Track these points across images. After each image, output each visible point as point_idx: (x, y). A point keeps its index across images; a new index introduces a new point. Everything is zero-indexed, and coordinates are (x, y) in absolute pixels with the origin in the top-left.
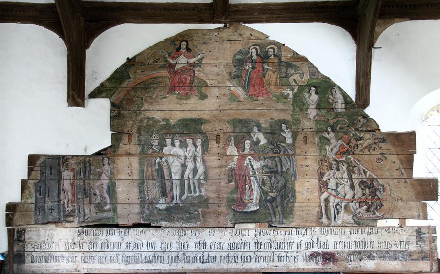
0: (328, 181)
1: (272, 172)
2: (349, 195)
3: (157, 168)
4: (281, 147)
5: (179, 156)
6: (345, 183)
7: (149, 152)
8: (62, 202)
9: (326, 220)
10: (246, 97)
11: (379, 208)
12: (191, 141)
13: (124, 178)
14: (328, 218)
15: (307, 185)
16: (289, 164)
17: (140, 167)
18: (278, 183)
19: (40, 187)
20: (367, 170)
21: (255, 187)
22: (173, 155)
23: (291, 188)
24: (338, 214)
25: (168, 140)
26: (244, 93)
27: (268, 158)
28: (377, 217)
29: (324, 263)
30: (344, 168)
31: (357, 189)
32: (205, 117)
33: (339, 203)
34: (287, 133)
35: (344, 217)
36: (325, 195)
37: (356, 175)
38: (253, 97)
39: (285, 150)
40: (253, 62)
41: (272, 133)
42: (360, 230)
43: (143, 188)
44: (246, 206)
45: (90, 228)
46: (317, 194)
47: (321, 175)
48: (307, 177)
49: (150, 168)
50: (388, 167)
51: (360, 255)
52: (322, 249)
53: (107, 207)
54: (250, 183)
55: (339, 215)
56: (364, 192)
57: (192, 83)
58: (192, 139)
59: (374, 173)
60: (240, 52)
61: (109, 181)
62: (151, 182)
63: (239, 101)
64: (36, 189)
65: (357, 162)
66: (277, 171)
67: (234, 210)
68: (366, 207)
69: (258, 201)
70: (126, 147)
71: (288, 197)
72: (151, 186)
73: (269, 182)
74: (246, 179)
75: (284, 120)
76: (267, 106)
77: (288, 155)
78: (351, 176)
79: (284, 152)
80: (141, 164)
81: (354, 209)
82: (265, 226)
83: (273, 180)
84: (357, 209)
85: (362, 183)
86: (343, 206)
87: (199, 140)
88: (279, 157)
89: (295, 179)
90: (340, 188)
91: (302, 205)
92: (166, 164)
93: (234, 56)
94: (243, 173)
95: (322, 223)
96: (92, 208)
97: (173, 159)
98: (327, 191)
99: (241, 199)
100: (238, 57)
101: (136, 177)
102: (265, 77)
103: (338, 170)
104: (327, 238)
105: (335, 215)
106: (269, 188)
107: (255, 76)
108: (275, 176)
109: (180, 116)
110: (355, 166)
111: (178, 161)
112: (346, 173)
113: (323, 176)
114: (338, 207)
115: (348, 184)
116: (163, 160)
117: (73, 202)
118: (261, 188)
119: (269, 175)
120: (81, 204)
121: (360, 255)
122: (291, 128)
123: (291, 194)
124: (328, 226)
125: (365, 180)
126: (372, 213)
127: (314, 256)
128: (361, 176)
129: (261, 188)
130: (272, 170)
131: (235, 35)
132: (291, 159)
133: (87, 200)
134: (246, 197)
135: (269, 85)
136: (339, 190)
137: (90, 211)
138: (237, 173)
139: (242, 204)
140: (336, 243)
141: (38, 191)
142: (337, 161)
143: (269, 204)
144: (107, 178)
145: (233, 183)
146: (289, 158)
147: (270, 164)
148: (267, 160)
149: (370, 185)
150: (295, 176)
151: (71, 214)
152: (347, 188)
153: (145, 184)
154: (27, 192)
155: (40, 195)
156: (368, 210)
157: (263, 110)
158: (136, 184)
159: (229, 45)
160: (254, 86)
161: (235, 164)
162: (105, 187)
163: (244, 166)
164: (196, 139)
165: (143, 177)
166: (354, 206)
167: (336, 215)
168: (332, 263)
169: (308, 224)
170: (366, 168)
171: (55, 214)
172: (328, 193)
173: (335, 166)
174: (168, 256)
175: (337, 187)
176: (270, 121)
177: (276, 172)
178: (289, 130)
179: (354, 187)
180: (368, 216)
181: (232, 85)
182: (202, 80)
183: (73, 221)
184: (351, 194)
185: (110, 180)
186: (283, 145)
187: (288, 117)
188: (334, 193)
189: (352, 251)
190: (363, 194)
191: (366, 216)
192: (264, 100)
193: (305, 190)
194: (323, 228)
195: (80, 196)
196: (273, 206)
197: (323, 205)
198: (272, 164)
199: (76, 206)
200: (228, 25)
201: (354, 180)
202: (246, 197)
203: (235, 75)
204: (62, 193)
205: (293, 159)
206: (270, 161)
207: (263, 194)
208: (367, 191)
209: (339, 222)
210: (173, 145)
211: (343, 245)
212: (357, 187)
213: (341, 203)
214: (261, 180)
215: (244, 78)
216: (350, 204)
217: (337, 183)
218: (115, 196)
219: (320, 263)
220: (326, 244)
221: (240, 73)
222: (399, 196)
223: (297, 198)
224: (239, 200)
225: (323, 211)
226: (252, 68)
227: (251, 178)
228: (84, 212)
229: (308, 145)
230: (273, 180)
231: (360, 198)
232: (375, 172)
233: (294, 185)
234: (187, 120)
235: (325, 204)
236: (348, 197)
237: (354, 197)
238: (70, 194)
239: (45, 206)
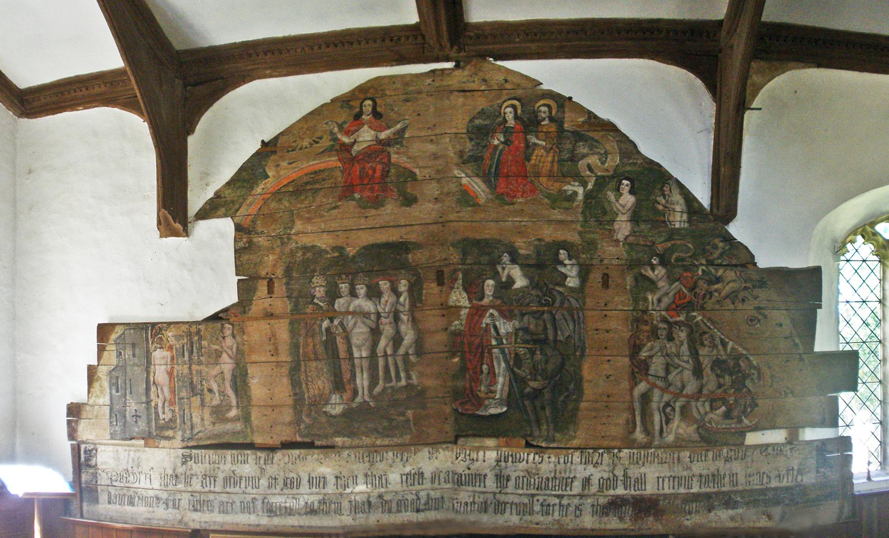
3: (324, 338)
4: (555, 293)
5: (366, 315)
6: (683, 364)
7: (308, 311)
8: (153, 404)
9: (643, 436)
10: (490, 196)
12: (388, 284)
13: (263, 359)
14: (647, 431)
15: (606, 368)
17: (292, 338)
19: (117, 377)
22: (354, 313)
24: (667, 423)
25: (343, 285)
26: (488, 190)
29: (636, 518)
32: (413, 238)
33: (672, 403)
34: (569, 267)
35: (679, 428)
36: (642, 387)
38: (502, 198)
39: (564, 298)
40: (507, 131)
41: (540, 266)
42: (710, 454)
43: (299, 377)
45: (203, 451)
46: (625, 385)
47: (635, 348)
48: (607, 352)
49: (310, 340)
51: (708, 501)
52: (633, 492)
53: (233, 413)
55: (670, 426)
57: (387, 176)
58: (390, 281)
60: (482, 113)
61: (235, 365)
62: (313, 364)
63: (476, 205)
64: (110, 381)
68: (723, 408)
70: (263, 303)
72: (314, 374)
75: (565, 241)
76: (532, 216)
77: (570, 310)
79: (562, 303)
80: (293, 333)
82: (518, 446)
84: (706, 413)
86: (677, 409)
87: (403, 282)
89: (583, 355)
91: (596, 405)
92: (341, 331)
93: (471, 121)
95: (635, 441)
96: (207, 416)
97: (354, 320)
100: (477, 122)
101: (285, 356)
102: (529, 160)
104: (643, 470)
107: (510, 158)
109: (368, 238)
111: (364, 323)
114: (668, 410)
116: (336, 322)
117: (172, 403)
120: (186, 407)
121: (708, 501)
122: (577, 258)
124: (647, 446)
126: (735, 420)
127: (615, 505)
131: (474, 82)
133: (196, 401)
135: (538, 175)
137: (202, 419)
140: (661, 480)
141: (114, 384)
144: (228, 360)
146: (573, 317)
151: (170, 425)
153: (303, 369)
154: (96, 385)
155: (118, 391)
157: (523, 223)
158: (285, 370)
159: (461, 100)
160: (507, 176)
162: (228, 376)
164: (398, 281)
165: (298, 356)
167: (664, 426)
168: (651, 518)
169: (606, 443)
171: (142, 425)
172: (648, 383)
174: (350, 502)
175: (667, 371)
176: (536, 243)
178: (574, 261)
181: (463, 175)
182: (405, 168)
183: (173, 438)
185: (237, 364)
186: (561, 289)
187: (573, 237)
188: (660, 383)
189: (693, 494)
191: (724, 426)
192: (526, 203)
193: (600, 375)
194: (635, 451)
195: (184, 394)
197: (637, 405)
199: (177, 410)
200: (462, 63)
203: (471, 156)
204: (153, 389)
205: (579, 317)
209: (671, 438)
210: (353, 294)
211: (676, 483)
213: (675, 402)
215: (488, 162)
216: (693, 404)
218: (246, 392)
219: (627, 519)
220: (641, 481)
221: (481, 152)
222: (788, 388)
223: (586, 392)
225: (638, 419)
226: (505, 143)
228: (191, 420)
229: (610, 291)
233: (580, 368)
234: (373, 246)
238: (166, 390)
239: (125, 411)
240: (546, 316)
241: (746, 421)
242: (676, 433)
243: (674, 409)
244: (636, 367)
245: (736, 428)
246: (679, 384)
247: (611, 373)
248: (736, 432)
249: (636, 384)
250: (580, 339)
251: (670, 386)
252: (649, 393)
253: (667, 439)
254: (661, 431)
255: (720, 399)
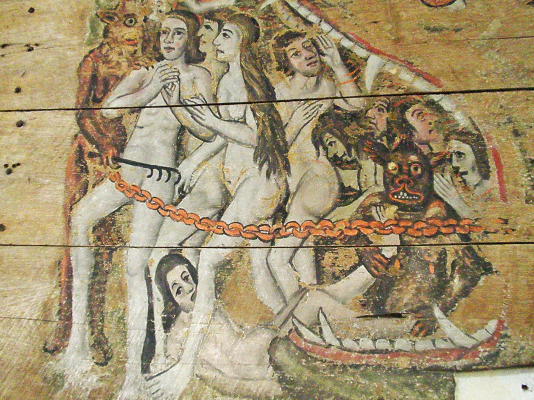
0: (128, 120)
2: (252, 201)
11: (457, 284)
14: (103, 351)
20: (361, 52)
24: (167, 325)
28: (444, 354)
30: (226, 45)
31: (305, 163)
33: (187, 253)
36: (102, 198)
37: (299, 79)
46: (55, 192)
48: (17, 102)
50: (494, 26)
56: (350, 178)
59: (409, 66)
65: (303, 11)
68: (362, 276)
78: (269, 89)
81: (279, 289)
84: (302, 291)
85: (333, 122)
86: (205, 274)
90: (197, 157)
95: (57, 381)
98: (117, 179)
103: (193, 56)
105: (151, 326)
110: (292, 36)
112: (236, 72)
113: (106, 91)
114: (175, 275)
115: (250, 132)
125: (356, 104)
128: (325, 88)
136: (186, 168)
142: (188, 14)
149: (389, 135)
152: (241, 159)
156: (377, 303)
166: (282, 267)
170: (359, 41)
172: (121, 186)
173: (178, 42)
175: (180, 151)
179: (282, 149)
180: (382, 344)
184: (262, 194)
188: (157, 188)
190: (343, 189)
191: (367, 344)
197: (82, 261)
201: (282, 109)
208: (370, 174)
212: (302, 148)
213: (198, 248)
216: (257, 256)
217: (182, 129)
231: (321, 219)
232: (417, 62)
235: (97, 254)
236: (240, 211)
237: (281, 212)
241: (451, 330)
242: (200, 361)
243: (194, 272)
244: (92, 141)
245: (412, 354)
246: (214, 194)
247: (16, 159)
248: (414, 371)
249: (84, 191)
251: (183, 194)
252: (118, 218)
253: (164, 382)
254: (149, 351)
255: (348, 242)
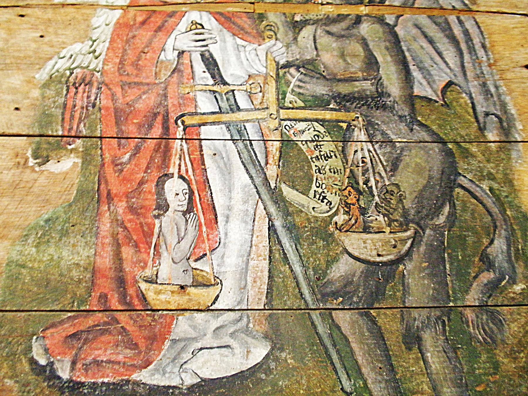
1: (344, 101)
16: (450, 55)
18: (394, 166)
21: (234, 191)
23: (489, 202)
27: (316, 22)
44: (156, 340)
54: (199, 163)
66: (381, 94)
67: (48, 373)
69: (256, 297)
71: (487, 263)
73: (336, 162)
74: (166, 137)
83: (361, 148)
88: (381, 20)
89: (507, 141)
94: (147, 101)
99: (121, 282)
106: (335, 200)
108: (369, 125)
118: (277, 197)
119: (328, 115)
123: (499, 245)
129: (277, 197)
130: (344, 89)
132: (457, 31)
134: (166, 269)
138: (104, 101)
139: (123, 317)
143: (344, 319)
145: (67, 164)
146: (447, 30)
147: (329, 59)
148: (307, 32)
150: (506, 127)
161: (102, 48)
163: (158, 62)
177: (377, 100)
196: (379, 335)
198: (342, 56)
202: (166, 269)
205: (466, 33)
206: (324, 40)
207: (297, 240)
214: (274, 147)
224: (106, 285)
227: (205, 132)
230: (361, 148)
233: (509, 182)
240: (365, 28)
250: (487, 93)
